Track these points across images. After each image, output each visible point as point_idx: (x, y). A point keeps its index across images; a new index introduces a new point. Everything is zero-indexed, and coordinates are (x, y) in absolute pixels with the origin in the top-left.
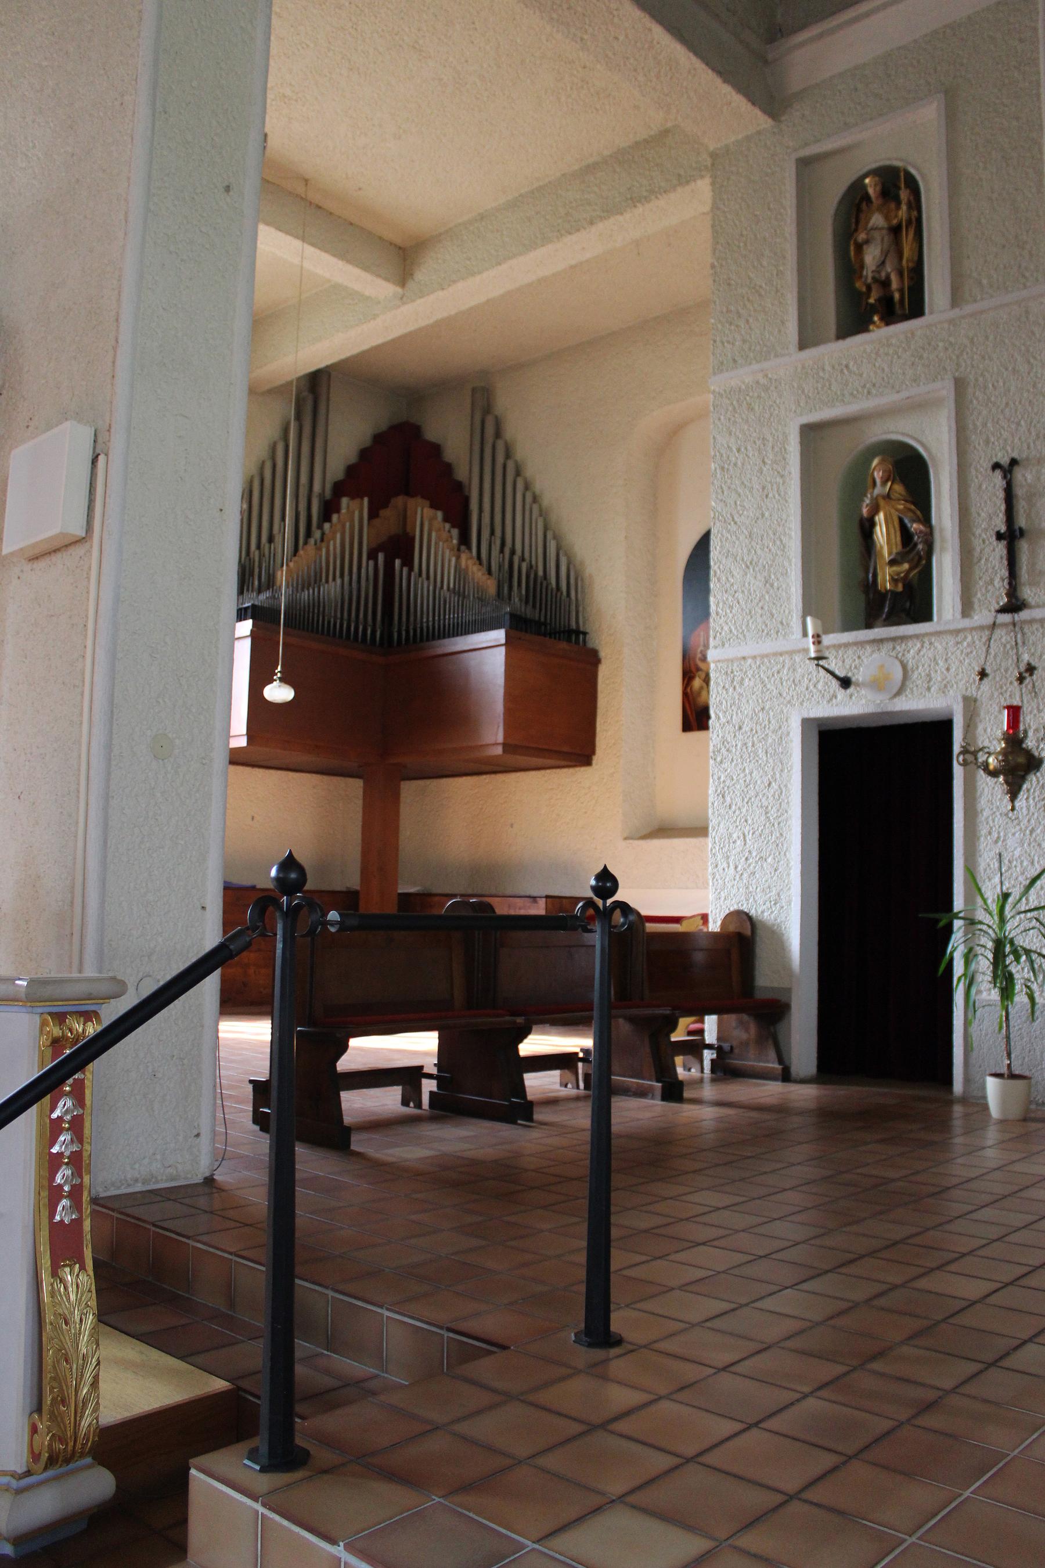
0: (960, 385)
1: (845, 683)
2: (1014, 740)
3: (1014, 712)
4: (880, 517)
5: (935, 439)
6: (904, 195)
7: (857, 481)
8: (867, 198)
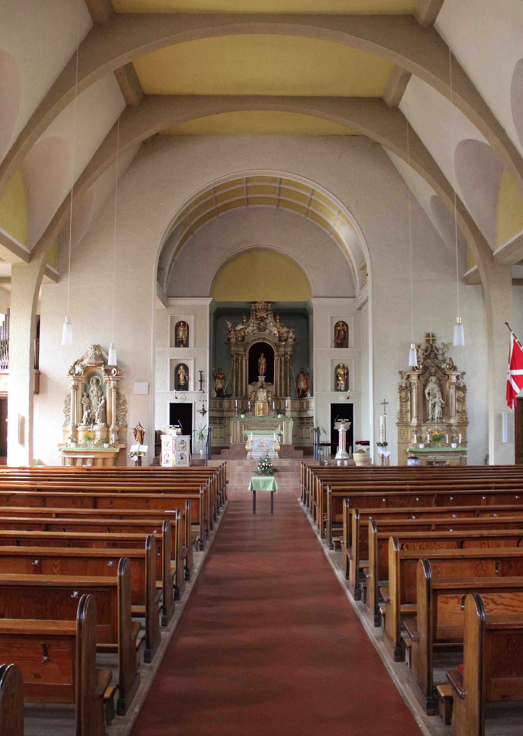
0: (195, 359)
1: (176, 398)
2: (203, 409)
3: (203, 405)
4: (181, 375)
5: (191, 365)
7: (177, 368)
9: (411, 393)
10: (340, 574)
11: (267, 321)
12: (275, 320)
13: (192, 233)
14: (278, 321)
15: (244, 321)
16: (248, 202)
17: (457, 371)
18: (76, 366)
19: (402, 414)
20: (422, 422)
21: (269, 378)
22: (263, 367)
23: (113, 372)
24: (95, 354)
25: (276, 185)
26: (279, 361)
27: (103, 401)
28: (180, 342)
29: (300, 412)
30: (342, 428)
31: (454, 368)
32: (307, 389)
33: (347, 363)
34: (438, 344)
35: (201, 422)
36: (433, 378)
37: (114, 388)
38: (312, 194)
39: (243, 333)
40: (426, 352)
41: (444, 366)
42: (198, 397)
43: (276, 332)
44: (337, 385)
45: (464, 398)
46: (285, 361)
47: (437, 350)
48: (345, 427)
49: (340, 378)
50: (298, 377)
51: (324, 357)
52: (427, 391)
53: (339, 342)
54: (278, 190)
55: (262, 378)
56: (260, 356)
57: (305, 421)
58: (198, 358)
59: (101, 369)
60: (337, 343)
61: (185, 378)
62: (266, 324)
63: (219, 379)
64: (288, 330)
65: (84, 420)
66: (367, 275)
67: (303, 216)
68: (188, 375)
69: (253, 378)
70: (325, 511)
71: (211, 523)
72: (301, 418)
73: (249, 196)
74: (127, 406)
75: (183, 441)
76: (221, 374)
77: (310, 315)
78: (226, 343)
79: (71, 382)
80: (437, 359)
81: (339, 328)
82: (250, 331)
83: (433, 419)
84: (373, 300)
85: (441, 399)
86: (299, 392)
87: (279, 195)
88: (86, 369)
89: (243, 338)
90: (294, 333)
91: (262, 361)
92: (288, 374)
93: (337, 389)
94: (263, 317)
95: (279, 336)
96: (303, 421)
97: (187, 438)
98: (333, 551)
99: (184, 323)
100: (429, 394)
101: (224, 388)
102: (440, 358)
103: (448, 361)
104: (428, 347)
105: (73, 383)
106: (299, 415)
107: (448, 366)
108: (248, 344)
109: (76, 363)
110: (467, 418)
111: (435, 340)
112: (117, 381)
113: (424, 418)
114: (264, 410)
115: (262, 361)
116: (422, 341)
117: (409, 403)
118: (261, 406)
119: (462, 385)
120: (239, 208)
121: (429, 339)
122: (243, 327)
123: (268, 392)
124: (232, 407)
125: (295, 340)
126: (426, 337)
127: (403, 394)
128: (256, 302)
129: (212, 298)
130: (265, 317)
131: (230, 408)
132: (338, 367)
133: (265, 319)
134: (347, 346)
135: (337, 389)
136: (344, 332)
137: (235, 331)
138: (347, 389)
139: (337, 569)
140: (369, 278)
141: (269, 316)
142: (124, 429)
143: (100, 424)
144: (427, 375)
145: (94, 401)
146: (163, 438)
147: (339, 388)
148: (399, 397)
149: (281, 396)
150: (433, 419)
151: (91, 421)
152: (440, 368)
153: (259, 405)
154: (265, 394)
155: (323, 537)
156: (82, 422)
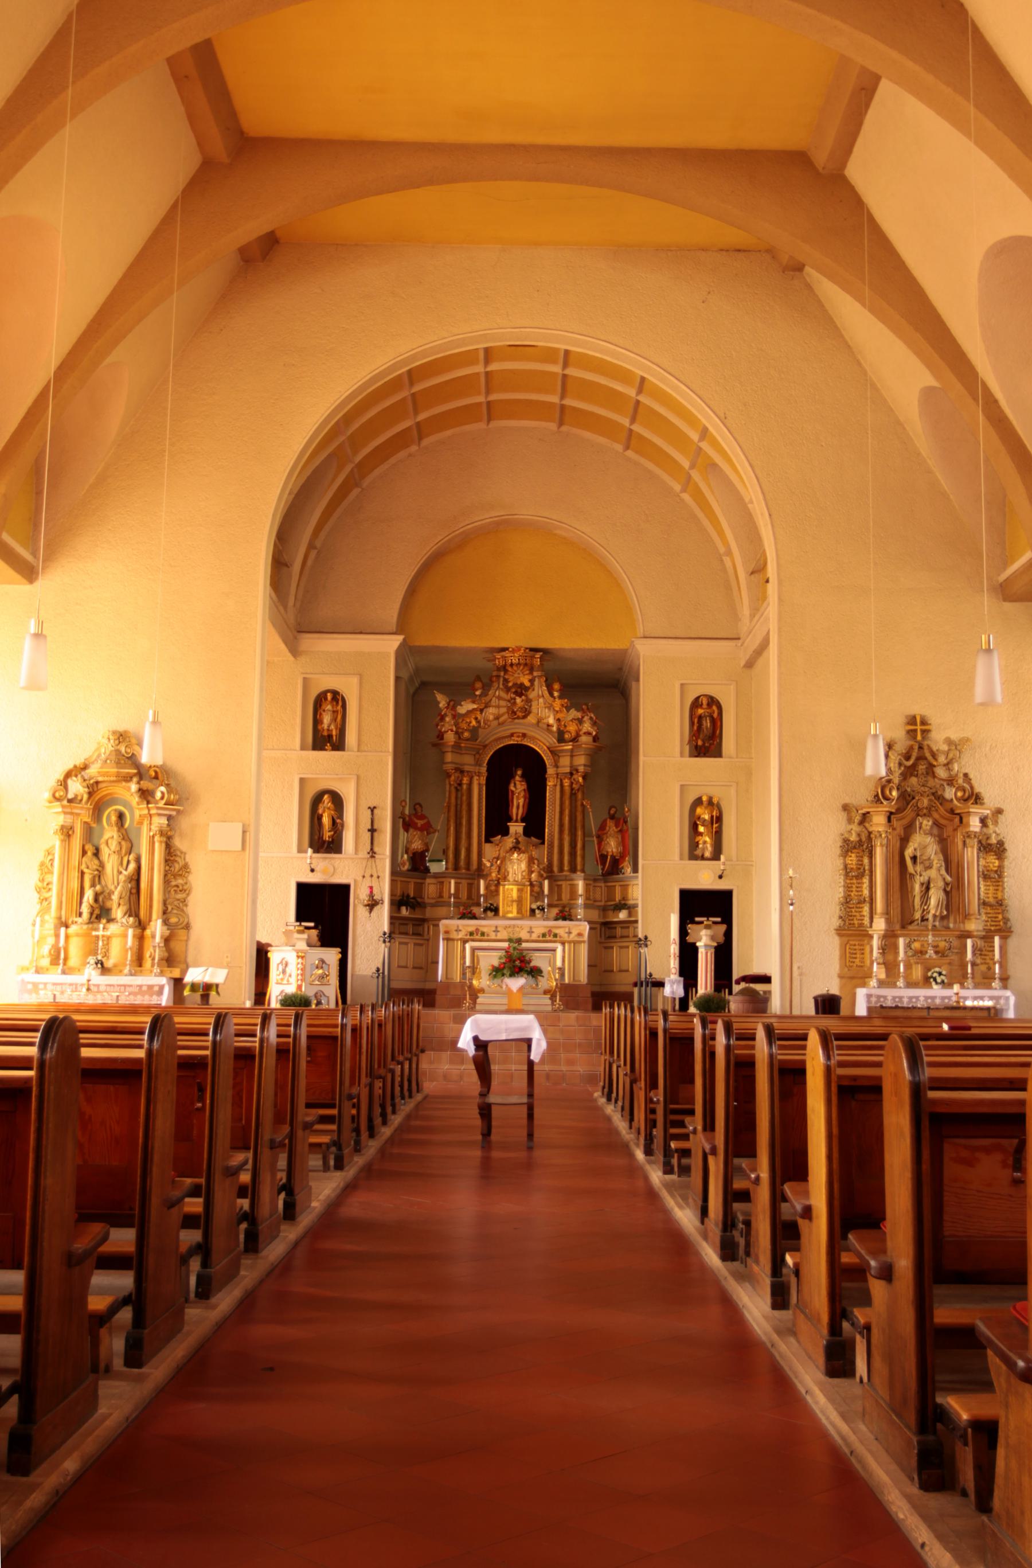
6: (340, 703)
7: (317, 799)
8: (326, 699)
9: (871, 856)
10: (686, 1217)
11: (532, 695)
12: (551, 694)
13: (357, 485)
14: (556, 694)
15: (478, 693)
16: (491, 411)
17: (982, 804)
18: (70, 782)
19: (850, 905)
20: (897, 927)
21: (535, 827)
22: (519, 802)
23: (158, 795)
24: (118, 752)
25: (557, 369)
26: (558, 788)
27: (132, 866)
28: (326, 739)
29: (604, 909)
30: (704, 939)
31: (977, 799)
32: (623, 856)
33: (717, 794)
34: (938, 739)
35: (369, 929)
36: (925, 822)
37: (162, 833)
38: (640, 391)
39: (474, 723)
40: (908, 758)
41: (949, 793)
42: (364, 870)
43: (551, 721)
44: (694, 845)
45: (1000, 872)
46: (572, 789)
47: (934, 755)
48: (713, 938)
49: (701, 829)
50: (602, 827)
51: (664, 777)
52: (909, 852)
53: (700, 743)
54: (559, 383)
55: (516, 828)
56: (513, 777)
57: (619, 931)
58: (367, 775)
59: (129, 789)
60: (696, 746)
61: (334, 823)
62: (529, 701)
63: (416, 828)
64: (579, 715)
65: (85, 909)
66: (767, 581)
67: (619, 447)
68: (341, 817)
69: (496, 825)
70: (653, 1085)
71: (370, 1120)
72: (608, 925)
73: (493, 397)
74: (191, 878)
75: (323, 961)
76: (422, 817)
77: (634, 684)
78: (435, 745)
79: (56, 817)
80: (934, 776)
81: (700, 711)
82: (491, 717)
83: (924, 919)
84: (780, 636)
85: (943, 872)
86: (603, 863)
87: (562, 398)
88: (93, 788)
89: (474, 731)
90: (594, 724)
91: (518, 788)
92: (579, 818)
93: (694, 853)
94: (522, 684)
95: (558, 729)
96: (611, 929)
97: (332, 955)
98: (674, 1177)
99: (335, 694)
100: (914, 859)
101: (427, 850)
102: (941, 773)
103: (960, 781)
104: (911, 748)
105: (61, 820)
106: (605, 917)
107: (959, 794)
108: (485, 746)
109: (68, 775)
110: (1006, 920)
111: (929, 731)
112: (169, 818)
113: (903, 918)
114: (520, 901)
115: (518, 788)
116: (899, 734)
117: (866, 880)
118: (515, 894)
119: (993, 840)
120: (467, 428)
121: (916, 730)
122: (475, 706)
123: (531, 861)
124: (445, 895)
125: (595, 739)
126: (909, 723)
127: (852, 859)
128: (507, 649)
129: (401, 638)
130: (527, 684)
131: (441, 896)
132: (698, 802)
133: (527, 689)
134: (719, 754)
135: (694, 853)
136: (713, 721)
137: (454, 717)
138: (716, 856)
139: (680, 1207)
140: (772, 589)
141: (536, 683)
142: (182, 933)
143: (124, 920)
144: (909, 813)
145: (111, 863)
146: (275, 958)
147: (698, 852)
148: (842, 867)
149: (561, 870)
150: (924, 919)
151: (101, 913)
152: (940, 799)
153: (510, 891)
154: (524, 866)
155: (648, 1152)
156: (80, 915)
